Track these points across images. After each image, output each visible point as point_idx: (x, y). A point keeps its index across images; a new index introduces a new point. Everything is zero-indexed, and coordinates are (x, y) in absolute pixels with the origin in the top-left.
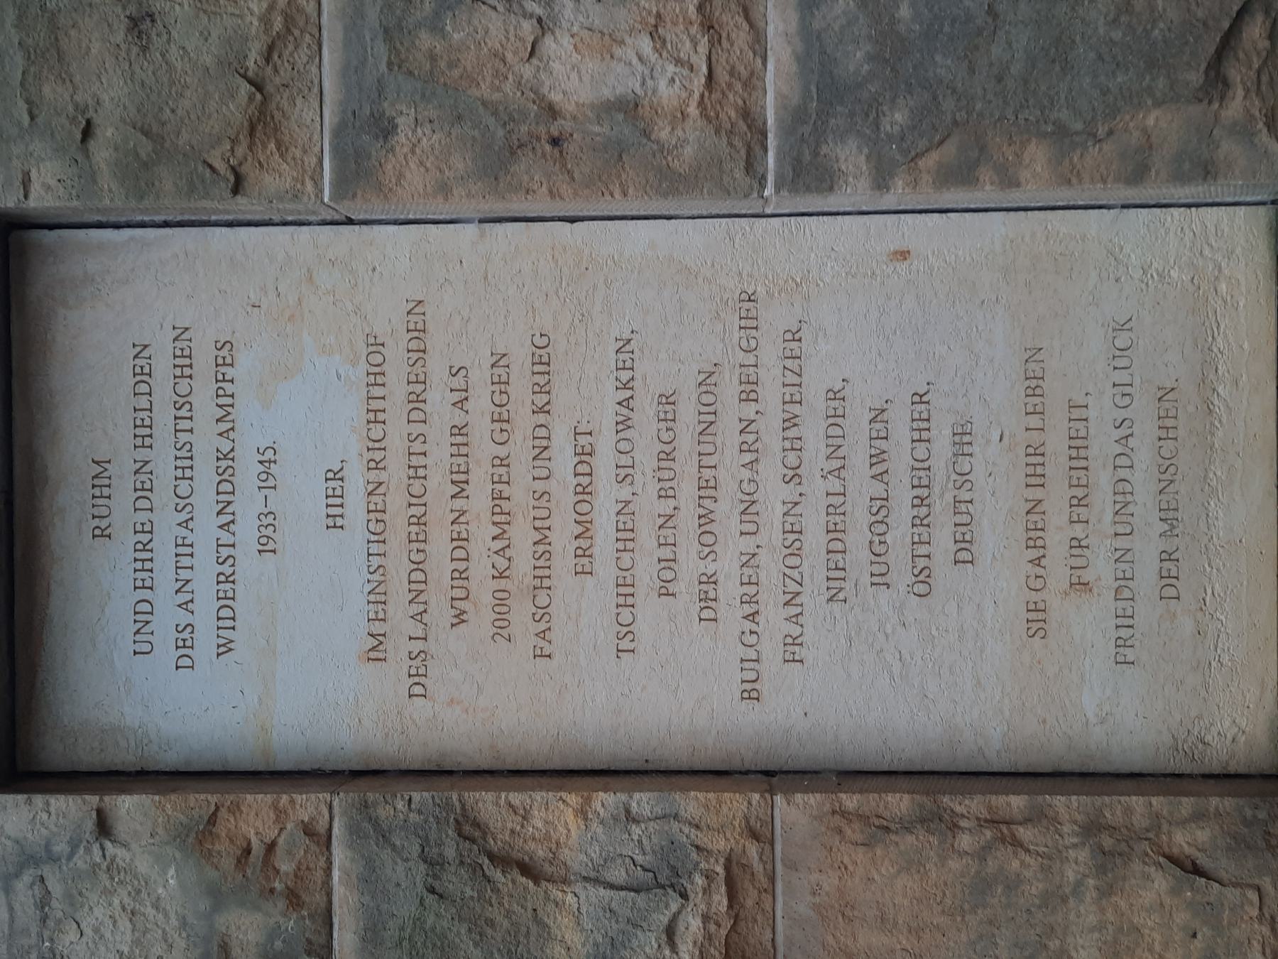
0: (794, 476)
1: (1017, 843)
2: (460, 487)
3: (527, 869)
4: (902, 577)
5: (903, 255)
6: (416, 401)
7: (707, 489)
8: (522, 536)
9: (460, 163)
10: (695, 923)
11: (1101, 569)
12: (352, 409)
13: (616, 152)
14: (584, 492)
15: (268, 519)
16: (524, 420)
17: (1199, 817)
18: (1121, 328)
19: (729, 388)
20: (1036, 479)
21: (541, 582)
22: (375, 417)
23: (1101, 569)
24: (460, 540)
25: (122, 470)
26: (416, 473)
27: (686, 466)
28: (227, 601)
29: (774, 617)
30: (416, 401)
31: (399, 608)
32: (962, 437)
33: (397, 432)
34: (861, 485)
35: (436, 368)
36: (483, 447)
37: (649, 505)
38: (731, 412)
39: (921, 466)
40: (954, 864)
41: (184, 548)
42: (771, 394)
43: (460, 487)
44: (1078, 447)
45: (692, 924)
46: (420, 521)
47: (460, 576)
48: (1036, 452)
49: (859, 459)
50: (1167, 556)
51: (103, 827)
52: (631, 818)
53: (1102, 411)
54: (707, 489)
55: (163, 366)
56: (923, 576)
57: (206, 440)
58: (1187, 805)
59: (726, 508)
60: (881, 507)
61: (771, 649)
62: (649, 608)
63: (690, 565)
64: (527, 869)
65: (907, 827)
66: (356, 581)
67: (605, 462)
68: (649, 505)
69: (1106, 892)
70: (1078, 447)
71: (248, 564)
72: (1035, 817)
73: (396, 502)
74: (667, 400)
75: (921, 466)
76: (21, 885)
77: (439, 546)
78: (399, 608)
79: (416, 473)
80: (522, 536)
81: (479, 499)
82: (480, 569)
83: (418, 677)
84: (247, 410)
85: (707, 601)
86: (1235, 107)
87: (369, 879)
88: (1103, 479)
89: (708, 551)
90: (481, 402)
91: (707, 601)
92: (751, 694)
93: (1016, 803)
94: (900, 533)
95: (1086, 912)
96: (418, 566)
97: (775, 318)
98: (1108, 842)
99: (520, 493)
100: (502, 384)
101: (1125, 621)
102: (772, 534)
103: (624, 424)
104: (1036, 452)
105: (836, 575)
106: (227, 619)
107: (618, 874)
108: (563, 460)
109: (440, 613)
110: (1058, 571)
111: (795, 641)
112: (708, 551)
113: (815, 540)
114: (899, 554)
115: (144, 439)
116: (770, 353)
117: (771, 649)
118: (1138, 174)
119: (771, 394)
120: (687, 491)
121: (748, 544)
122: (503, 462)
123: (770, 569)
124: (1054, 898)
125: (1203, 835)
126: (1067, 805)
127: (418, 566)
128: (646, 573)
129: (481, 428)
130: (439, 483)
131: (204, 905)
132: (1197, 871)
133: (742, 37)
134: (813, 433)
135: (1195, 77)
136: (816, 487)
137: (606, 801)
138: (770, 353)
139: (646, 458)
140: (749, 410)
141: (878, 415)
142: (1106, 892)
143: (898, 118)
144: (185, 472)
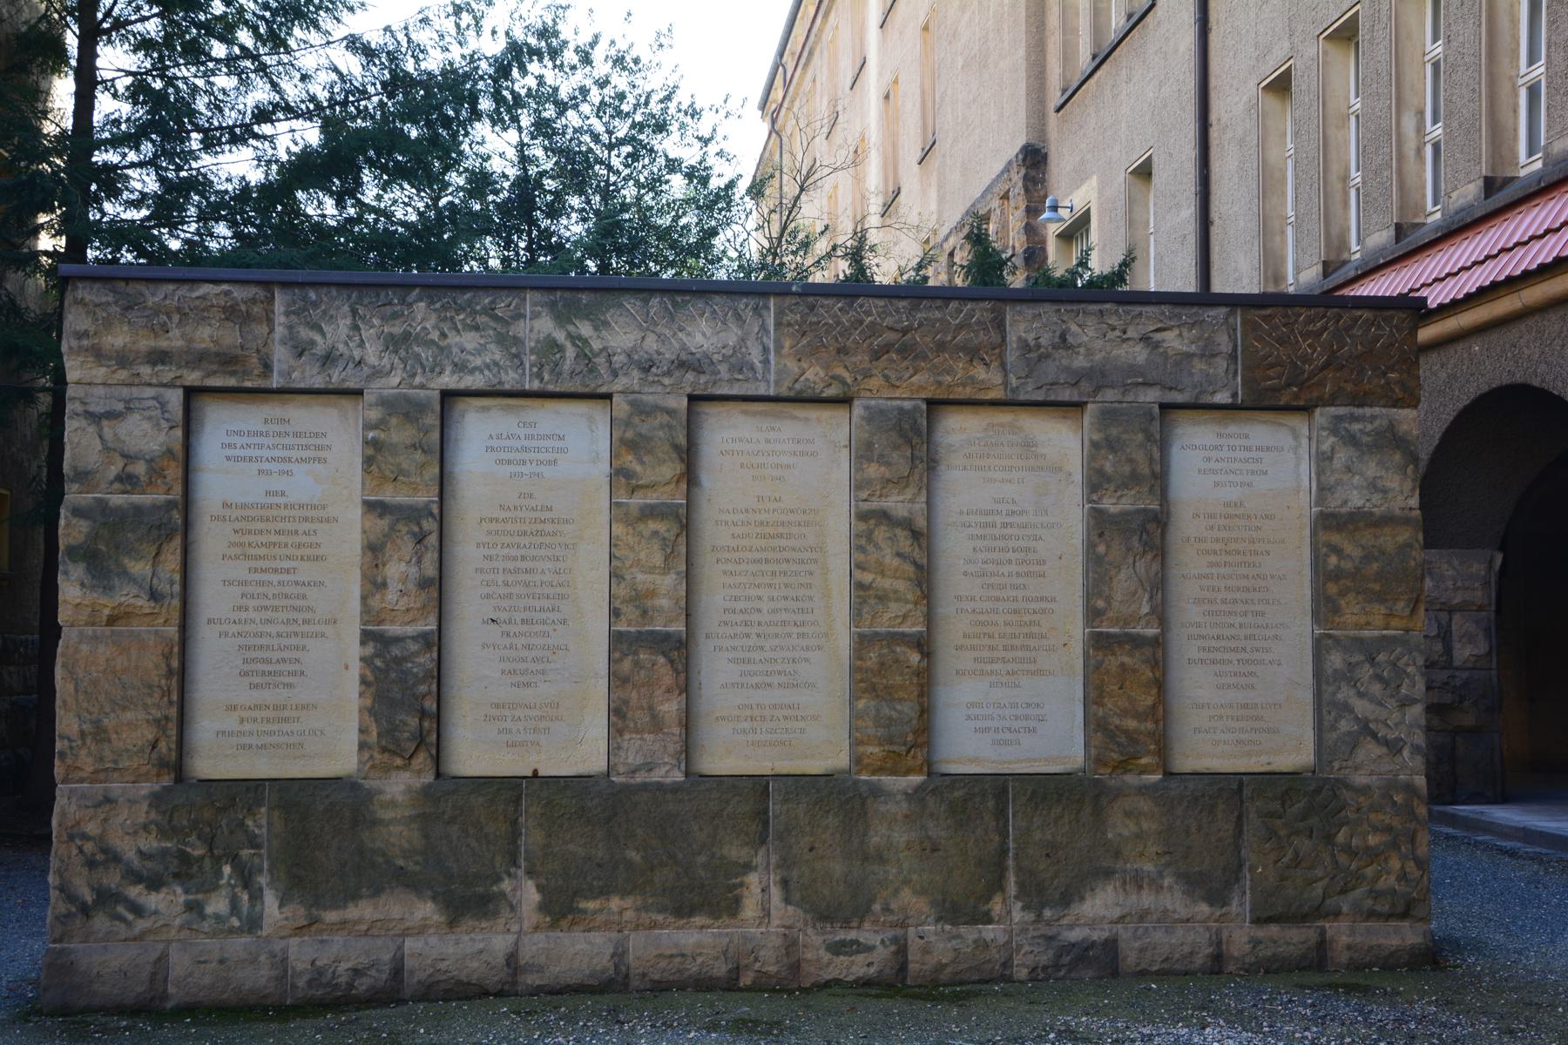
0: (279, 635)
1: (163, 696)
2: (278, 533)
3: (157, 554)
4: (247, 667)
5: (347, 668)
6: (306, 519)
7: (275, 609)
8: (262, 551)
9: (372, 537)
10: (140, 604)
11: (247, 727)
13: (374, 583)
14: (276, 571)
15: (269, 473)
16: (299, 553)
17: (170, 749)
18: (322, 733)
19: (308, 616)
20: (276, 708)
21: (248, 557)
22: (301, 506)
23: (247, 727)
24: (261, 532)
25: (287, 428)
26: (283, 519)
27: (284, 602)
28: (244, 459)
29: (235, 628)
30: (306, 519)
32: (290, 686)
33: (296, 513)
34: (276, 655)
36: (290, 540)
37: (271, 591)
38: (300, 616)
39: (281, 673)
40: (156, 679)
41: (261, 446)
42: (306, 628)
43: (278, 533)
44: (286, 720)
45: (140, 602)
46: (268, 520)
47: (250, 532)
48: (285, 707)
49: (285, 655)
50: (250, 746)
52: (171, 585)
53: (296, 727)
54: (275, 609)
55: (319, 441)
56: (246, 674)
57: (294, 454)
58: (173, 746)
59: (269, 614)
60: (269, 661)
61: (225, 628)
62: (238, 590)
63: (252, 603)
64: (157, 554)
65: (168, 665)
67: (285, 577)
68: (271, 591)
69: (148, 721)
70: (286, 720)
71: (255, 466)
72: (171, 703)
73: (275, 512)
74: (304, 597)
75: (281, 673)
76: (154, 403)
77: (260, 526)
78: (239, 513)
79: (283, 519)
80: (262, 551)
81: (273, 538)
82: (252, 538)
83: (218, 518)
84: (305, 467)
85: (240, 608)
86: (377, 755)
87: (155, 507)
88: (275, 727)
89: (256, 609)
90: (304, 539)
91: (240, 608)
92: (210, 621)
93: (175, 698)
94: (260, 667)
95: (141, 715)
96: (253, 519)
97: (329, 630)
98: (163, 722)
99: (276, 551)
101: (231, 734)
102: (261, 628)
103: (297, 583)
104: (285, 707)
105: (248, 648)
106: (237, 459)
107: (155, 581)
108: (286, 564)
109: (238, 525)
110: (245, 714)
111: (226, 634)
112: (256, 609)
113: (259, 641)
114: (253, 667)
115: (296, 435)
116: (317, 628)
117: (225, 628)
118: (361, 731)
119: (306, 628)
120: (276, 603)
121: (258, 621)
122: (286, 545)
123: (250, 628)
124: (145, 707)
125: (164, 750)
126: (173, 712)
127: (253, 519)
128: (250, 589)
129: (298, 539)
130: (281, 526)
131: (147, 457)
132: (154, 747)
133: (407, 619)
134: (293, 641)
135: (384, 743)
136: (275, 642)
137: (177, 577)
138: (317, 628)
139: (287, 590)
140: (300, 622)
141: (297, 661)
142: (148, 721)
143: (378, 663)
144: (285, 447)
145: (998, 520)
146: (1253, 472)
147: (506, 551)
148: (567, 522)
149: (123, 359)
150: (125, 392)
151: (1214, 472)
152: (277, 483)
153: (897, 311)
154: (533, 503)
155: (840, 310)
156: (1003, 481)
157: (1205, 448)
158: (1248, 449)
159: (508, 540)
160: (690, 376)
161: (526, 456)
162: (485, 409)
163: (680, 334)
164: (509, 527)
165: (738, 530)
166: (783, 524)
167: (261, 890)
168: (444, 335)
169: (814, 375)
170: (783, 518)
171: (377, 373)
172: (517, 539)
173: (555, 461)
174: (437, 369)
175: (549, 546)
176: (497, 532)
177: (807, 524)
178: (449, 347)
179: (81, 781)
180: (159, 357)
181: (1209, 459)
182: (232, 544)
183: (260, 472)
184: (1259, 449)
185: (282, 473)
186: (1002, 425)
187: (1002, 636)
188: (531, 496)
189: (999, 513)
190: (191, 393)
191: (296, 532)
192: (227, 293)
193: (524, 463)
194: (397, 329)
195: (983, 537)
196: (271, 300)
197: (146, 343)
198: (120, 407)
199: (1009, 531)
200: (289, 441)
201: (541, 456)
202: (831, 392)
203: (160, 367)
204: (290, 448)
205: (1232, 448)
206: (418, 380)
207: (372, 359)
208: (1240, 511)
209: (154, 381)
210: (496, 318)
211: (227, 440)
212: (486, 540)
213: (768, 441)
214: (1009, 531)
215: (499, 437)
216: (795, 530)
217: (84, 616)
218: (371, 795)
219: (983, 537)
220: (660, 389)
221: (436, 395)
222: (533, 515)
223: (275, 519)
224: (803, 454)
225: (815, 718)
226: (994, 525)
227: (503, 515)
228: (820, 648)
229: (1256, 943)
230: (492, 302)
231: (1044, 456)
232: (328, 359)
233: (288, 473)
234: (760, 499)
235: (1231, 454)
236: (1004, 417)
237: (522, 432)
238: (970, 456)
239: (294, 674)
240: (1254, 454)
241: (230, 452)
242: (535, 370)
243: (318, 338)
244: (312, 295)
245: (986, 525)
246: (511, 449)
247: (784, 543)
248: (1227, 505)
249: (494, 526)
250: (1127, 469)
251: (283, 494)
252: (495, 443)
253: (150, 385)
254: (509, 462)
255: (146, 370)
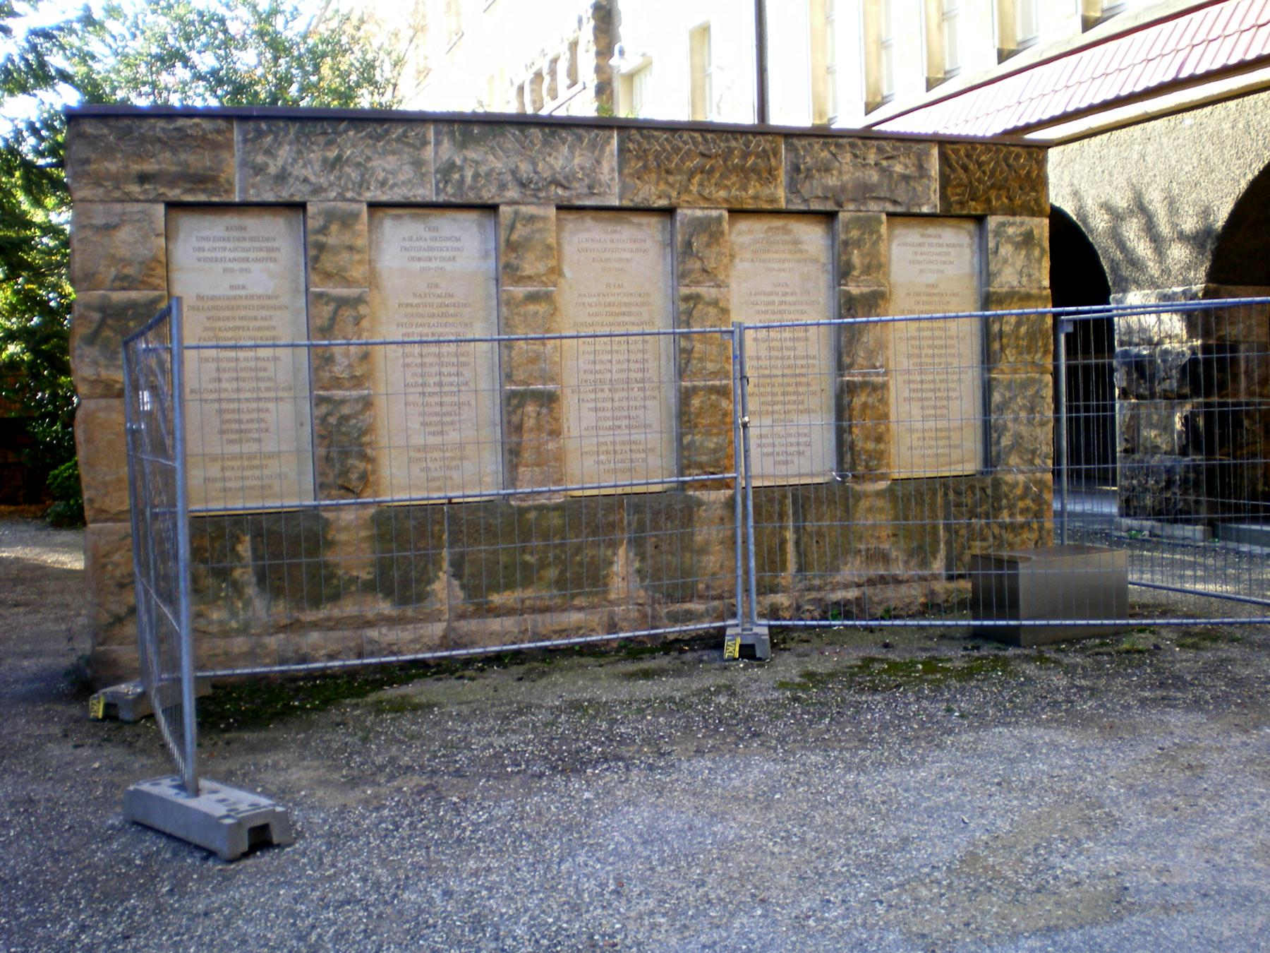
2: (242, 318)
6: (263, 307)
12: (260, 291)
15: (232, 270)
22: (259, 297)
24: (228, 319)
25: (243, 234)
26: (245, 307)
28: (211, 260)
30: (263, 307)
31: (210, 303)
33: (256, 303)
35: (272, 313)
36: (251, 324)
41: (224, 249)
43: (242, 318)
47: (219, 319)
51: (158, 235)
55: (270, 245)
57: (252, 255)
66: (217, 292)
71: (221, 266)
73: (239, 302)
77: (228, 313)
78: (210, 303)
79: (245, 307)
81: (239, 323)
82: (221, 324)
84: (261, 265)
90: (263, 323)
100: (268, 328)
109: (212, 313)
115: (253, 239)
129: (258, 323)
130: (243, 313)
131: (140, 259)
144: (243, 250)
145: (776, 299)
146: (944, 262)
147: (420, 329)
148: (465, 305)
149: (118, 180)
150: (118, 207)
151: (920, 262)
152: (240, 280)
153: (706, 140)
154: (438, 291)
155: (667, 139)
156: (779, 270)
157: (913, 245)
158: (941, 245)
159: (420, 320)
160: (560, 191)
161: (431, 254)
162: (399, 217)
163: (548, 159)
164: (421, 310)
165: (592, 310)
166: (625, 304)
167: (251, 598)
168: (369, 159)
169: (651, 192)
170: (625, 299)
171: (317, 190)
172: (427, 320)
173: (454, 258)
174: (365, 186)
175: (452, 325)
176: (412, 315)
177: (643, 304)
178: (372, 168)
179: (106, 520)
180: (143, 178)
181: (916, 253)
182: (207, 329)
183: (225, 270)
184: (948, 245)
185: (242, 270)
186: (778, 228)
187: (781, 385)
188: (437, 286)
189: (777, 294)
190: (172, 206)
191: (256, 318)
192: (197, 125)
193: (430, 259)
194: (332, 154)
195: (766, 312)
196: (231, 130)
197: (136, 168)
198: (117, 220)
199: (783, 307)
200: (246, 244)
201: (444, 254)
202: (663, 202)
203: (147, 187)
204: (248, 250)
205: (931, 245)
206: (349, 195)
207: (313, 179)
208: (935, 291)
209: (141, 197)
210: (408, 145)
211: (197, 244)
212: (405, 320)
213: (612, 241)
214: (783, 307)
215: (411, 239)
216: (634, 309)
217: (99, 390)
218: (327, 524)
219: (766, 312)
220: (535, 200)
221: (365, 208)
222: (440, 300)
223: (238, 308)
224: (638, 250)
225: (653, 450)
226: (773, 303)
227: (416, 301)
228: (654, 398)
229: (948, 592)
230: (405, 132)
231: (807, 251)
232: (282, 177)
233: (247, 271)
234: (608, 285)
235: (931, 250)
236: (778, 223)
237: (428, 235)
238: (755, 252)
239: (259, 430)
240: (945, 249)
241: (201, 255)
242: (441, 186)
243: (271, 162)
244: (264, 126)
245: (768, 303)
246: (420, 249)
247: (626, 319)
248: (928, 286)
249: (410, 310)
250: (867, 261)
251: (244, 287)
252: (407, 244)
253: (138, 201)
254: (419, 259)
255: (135, 189)
